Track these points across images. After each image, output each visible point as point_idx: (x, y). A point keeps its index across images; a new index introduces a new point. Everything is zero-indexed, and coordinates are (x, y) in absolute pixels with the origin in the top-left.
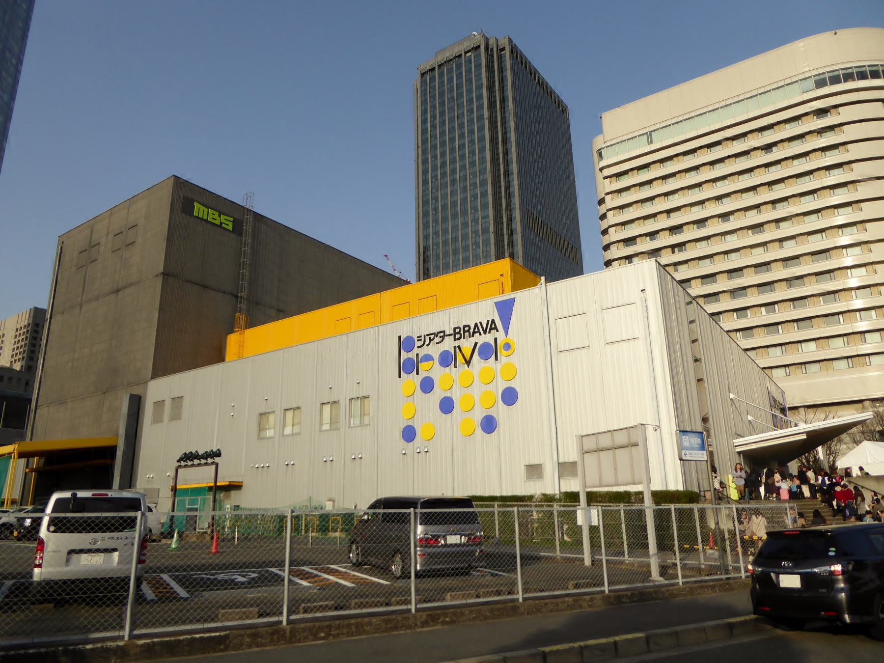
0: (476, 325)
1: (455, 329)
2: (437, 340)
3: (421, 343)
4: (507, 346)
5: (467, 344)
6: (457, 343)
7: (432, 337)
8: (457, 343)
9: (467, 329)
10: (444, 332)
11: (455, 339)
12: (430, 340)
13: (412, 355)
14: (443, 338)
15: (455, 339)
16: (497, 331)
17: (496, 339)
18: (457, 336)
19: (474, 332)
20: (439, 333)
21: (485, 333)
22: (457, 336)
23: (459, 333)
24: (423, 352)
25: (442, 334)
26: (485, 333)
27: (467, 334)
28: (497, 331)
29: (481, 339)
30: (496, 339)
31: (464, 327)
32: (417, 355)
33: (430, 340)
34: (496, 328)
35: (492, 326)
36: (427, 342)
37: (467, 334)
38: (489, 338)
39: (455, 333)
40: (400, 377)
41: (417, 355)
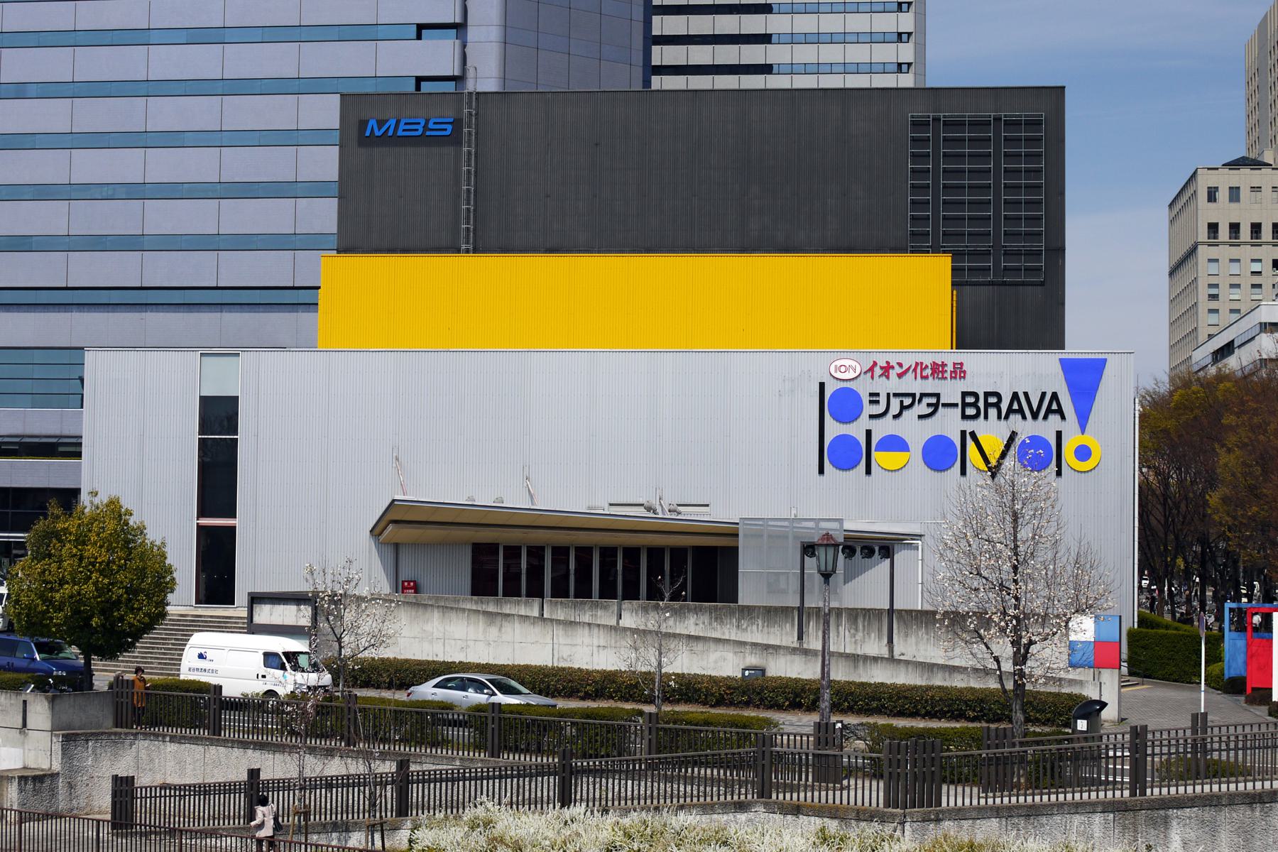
0: (1015, 396)
1: (964, 394)
2: (923, 409)
3: (880, 409)
4: (1083, 453)
5: (992, 433)
6: (969, 426)
7: (907, 401)
8: (969, 426)
9: (992, 400)
10: (937, 396)
11: (964, 417)
12: (903, 408)
13: (856, 431)
14: (936, 407)
15: (964, 417)
16: (1063, 418)
17: (1059, 434)
18: (970, 411)
19: (1010, 411)
20: (922, 395)
21: (1035, 416)
22: (970, 411)
23: (975, 405)
24: (882, 429)
25: (934, 400)
26: (1035, 416)
27: (993, 412)
28: (1063, 418)
29: (1026, 428)
30: (1059, 434)
31: (987, 395)
32: (869, 433)
33: (903, 408)
34: (1060, 412)
35: (1053, 407)
36: (895, 409)
37: (993, 412)
38: (1046, 429)
39: (965, 405)
40: (821, 471)
41: (869, 433)
